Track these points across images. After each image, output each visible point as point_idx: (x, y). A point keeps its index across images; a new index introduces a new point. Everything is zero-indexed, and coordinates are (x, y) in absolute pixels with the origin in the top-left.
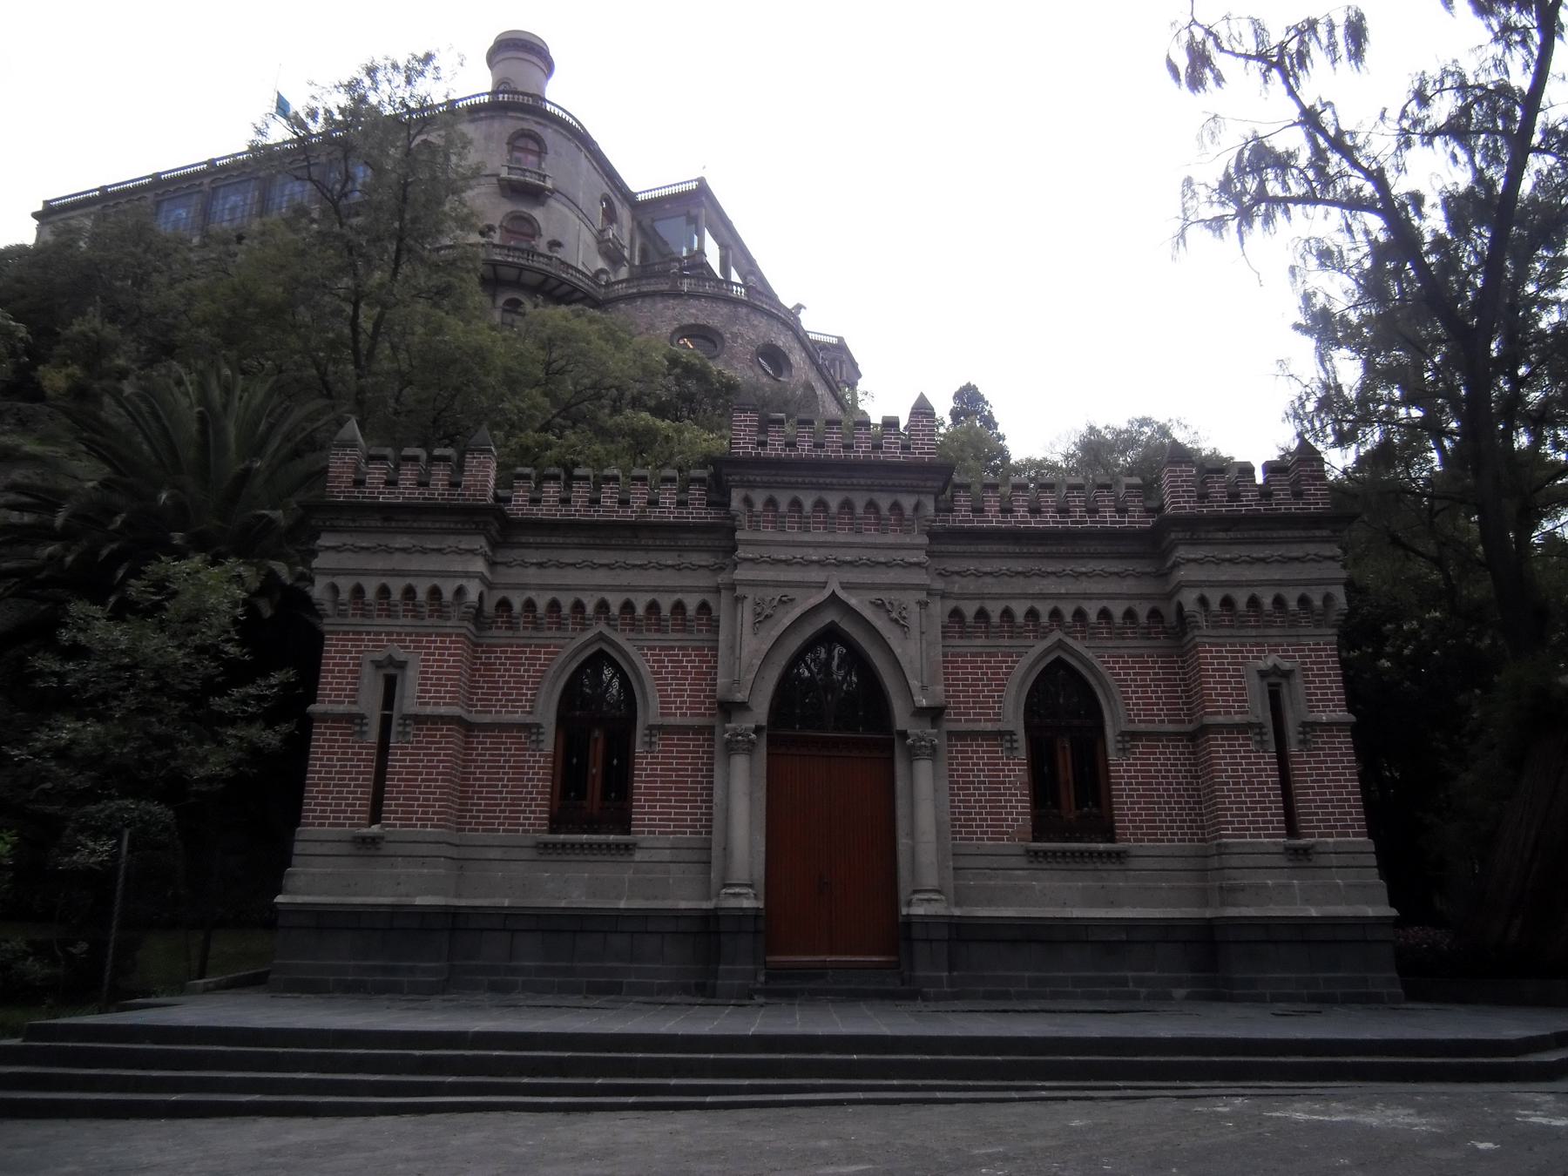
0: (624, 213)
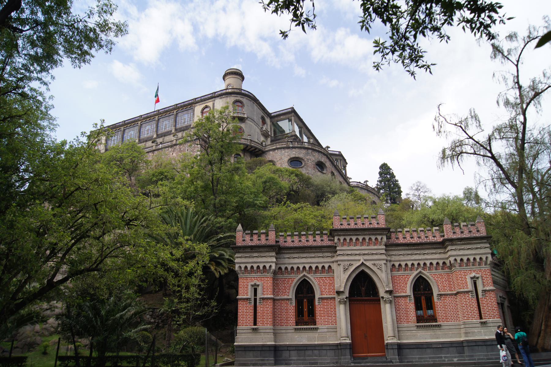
0: (268, 120)
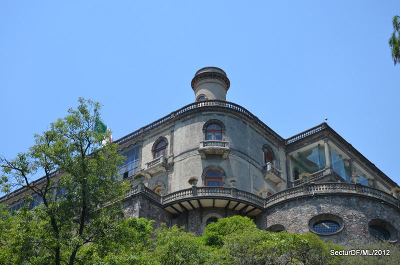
0: (280, 154)
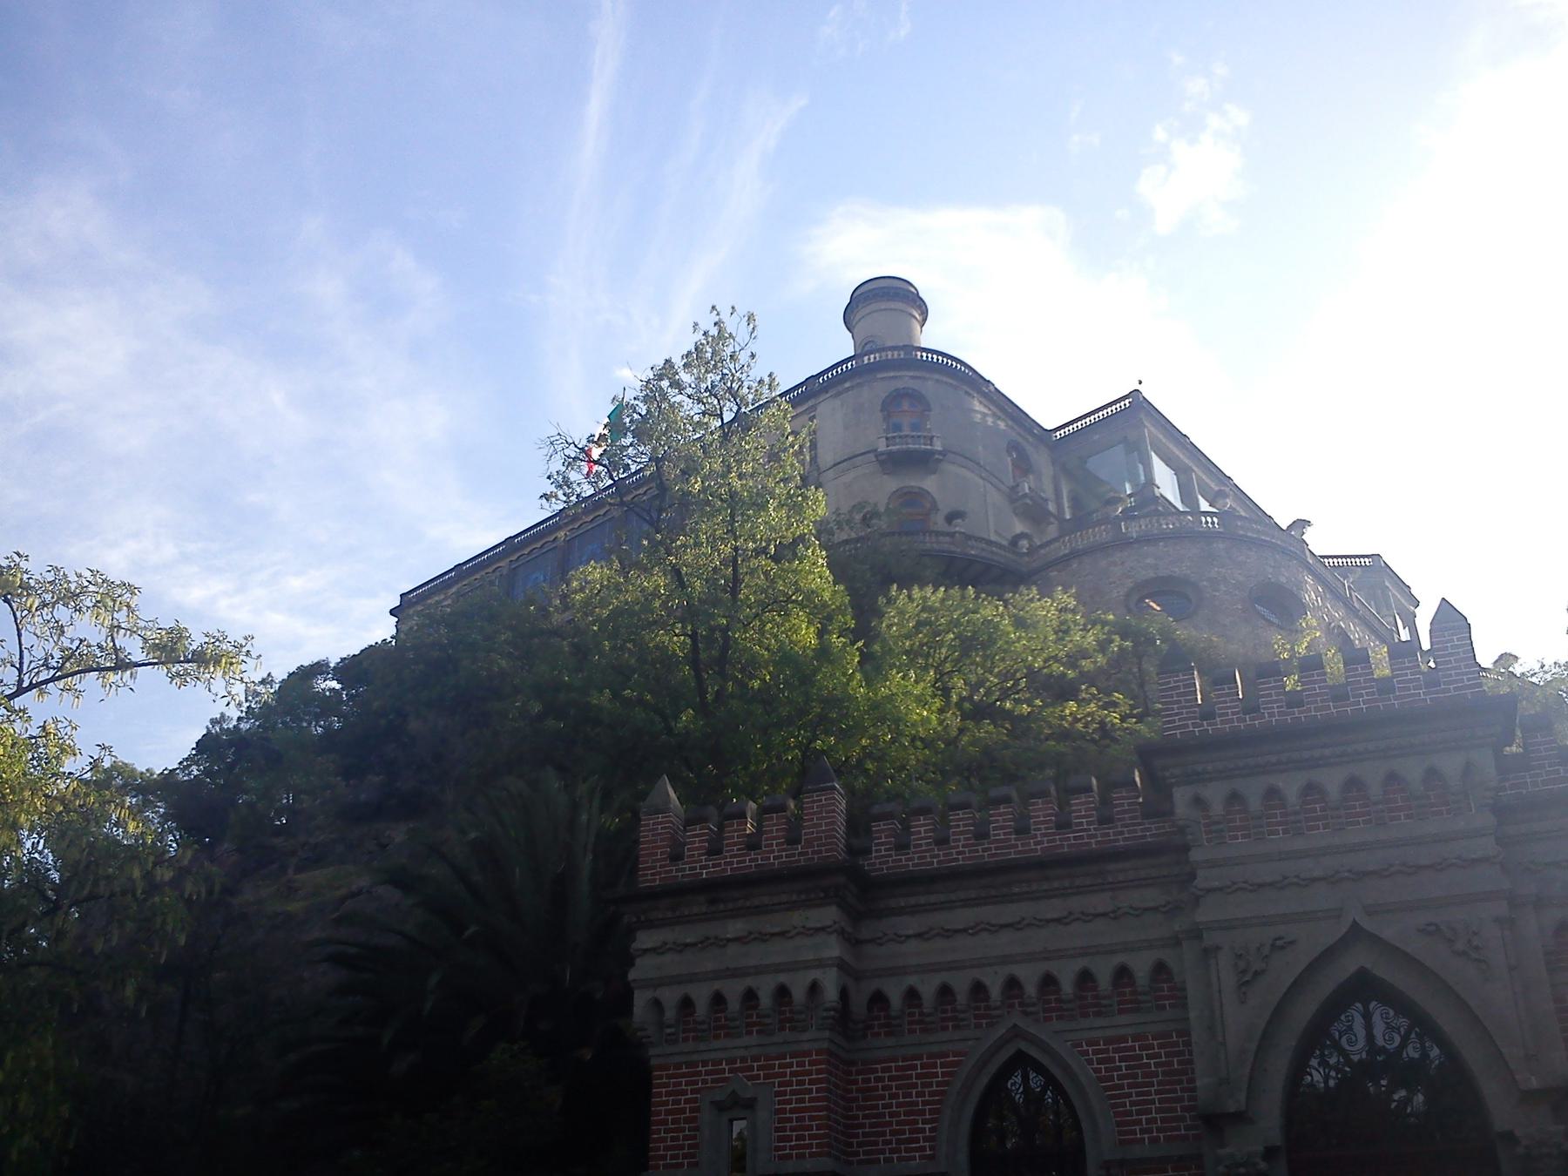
0: (1041, 459)
